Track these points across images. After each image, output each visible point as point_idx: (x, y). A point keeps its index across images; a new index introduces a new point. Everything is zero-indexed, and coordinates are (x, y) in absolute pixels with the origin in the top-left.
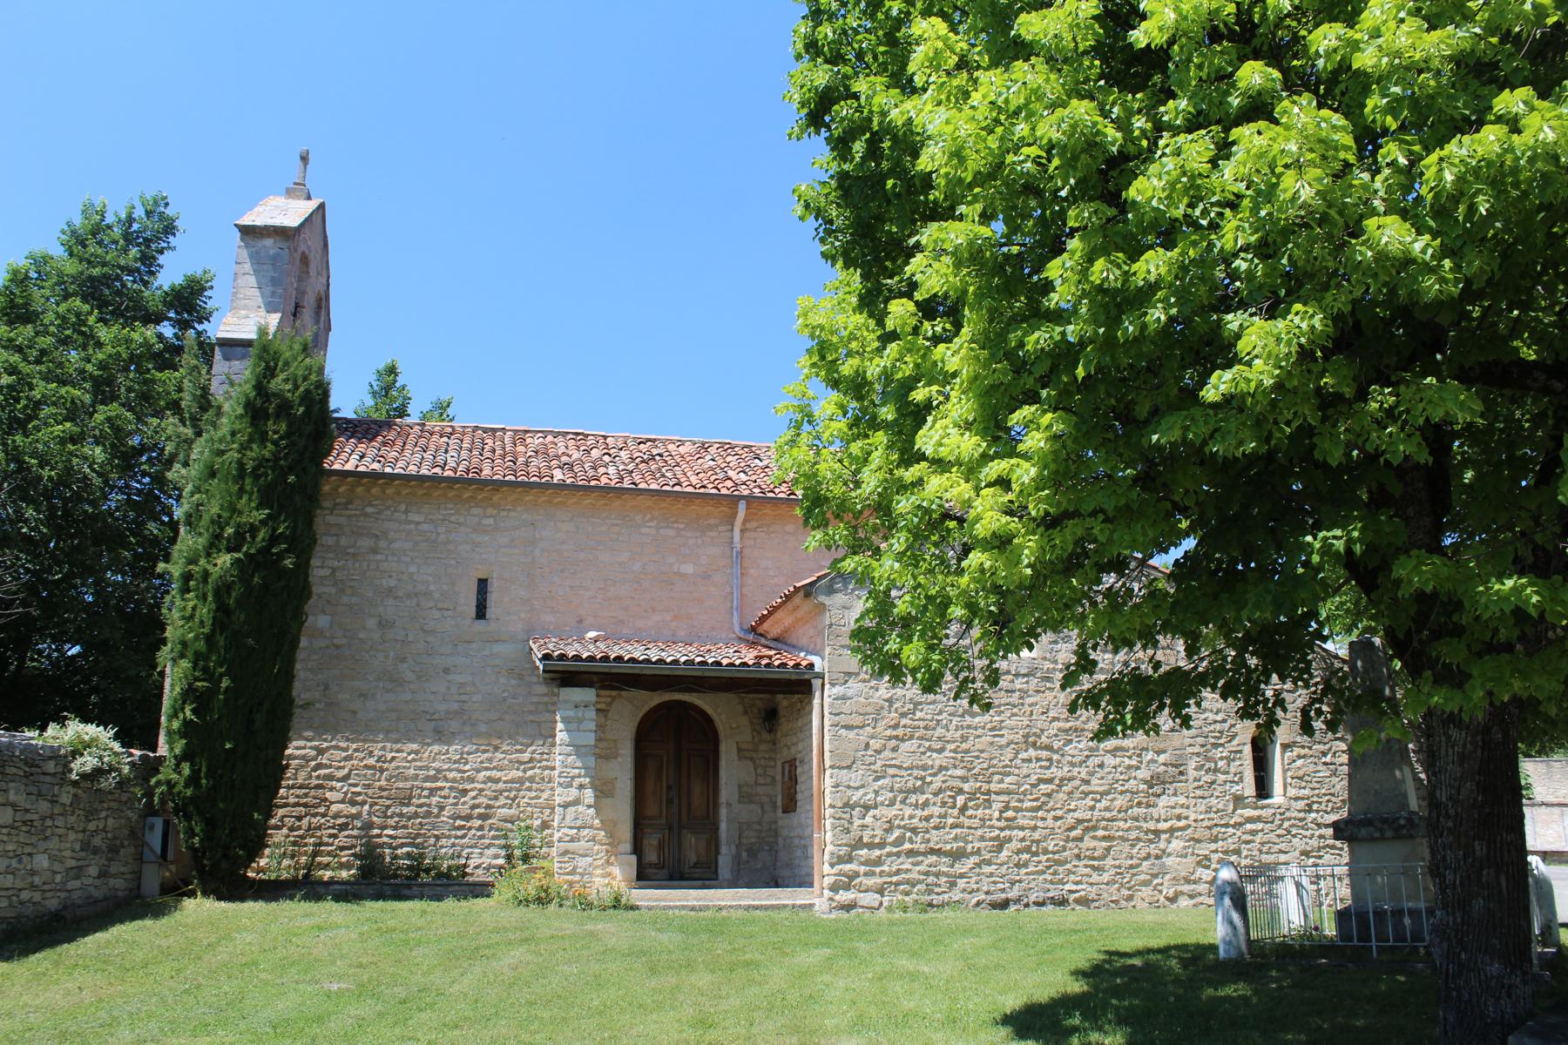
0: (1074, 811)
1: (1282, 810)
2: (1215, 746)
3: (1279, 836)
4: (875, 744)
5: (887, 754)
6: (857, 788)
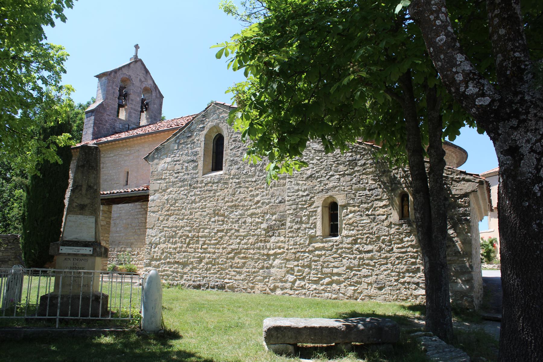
0: (231, 245)
1: (337, 243)
2: (302, 209)
3: (334, 258)
4: (161, 218)
5: (165, 222)
6: (154, 237)
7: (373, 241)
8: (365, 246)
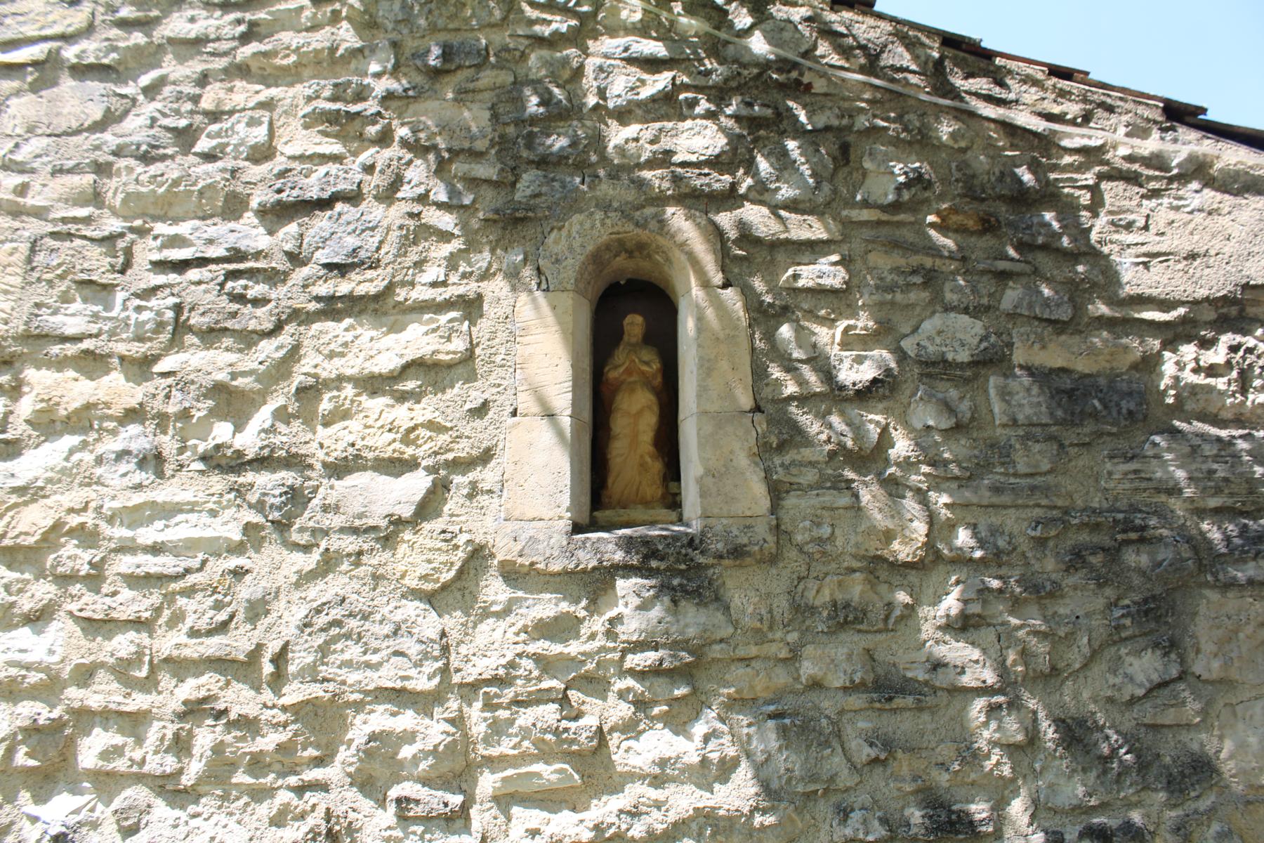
7: (257, 764)
8: (161, 809)
